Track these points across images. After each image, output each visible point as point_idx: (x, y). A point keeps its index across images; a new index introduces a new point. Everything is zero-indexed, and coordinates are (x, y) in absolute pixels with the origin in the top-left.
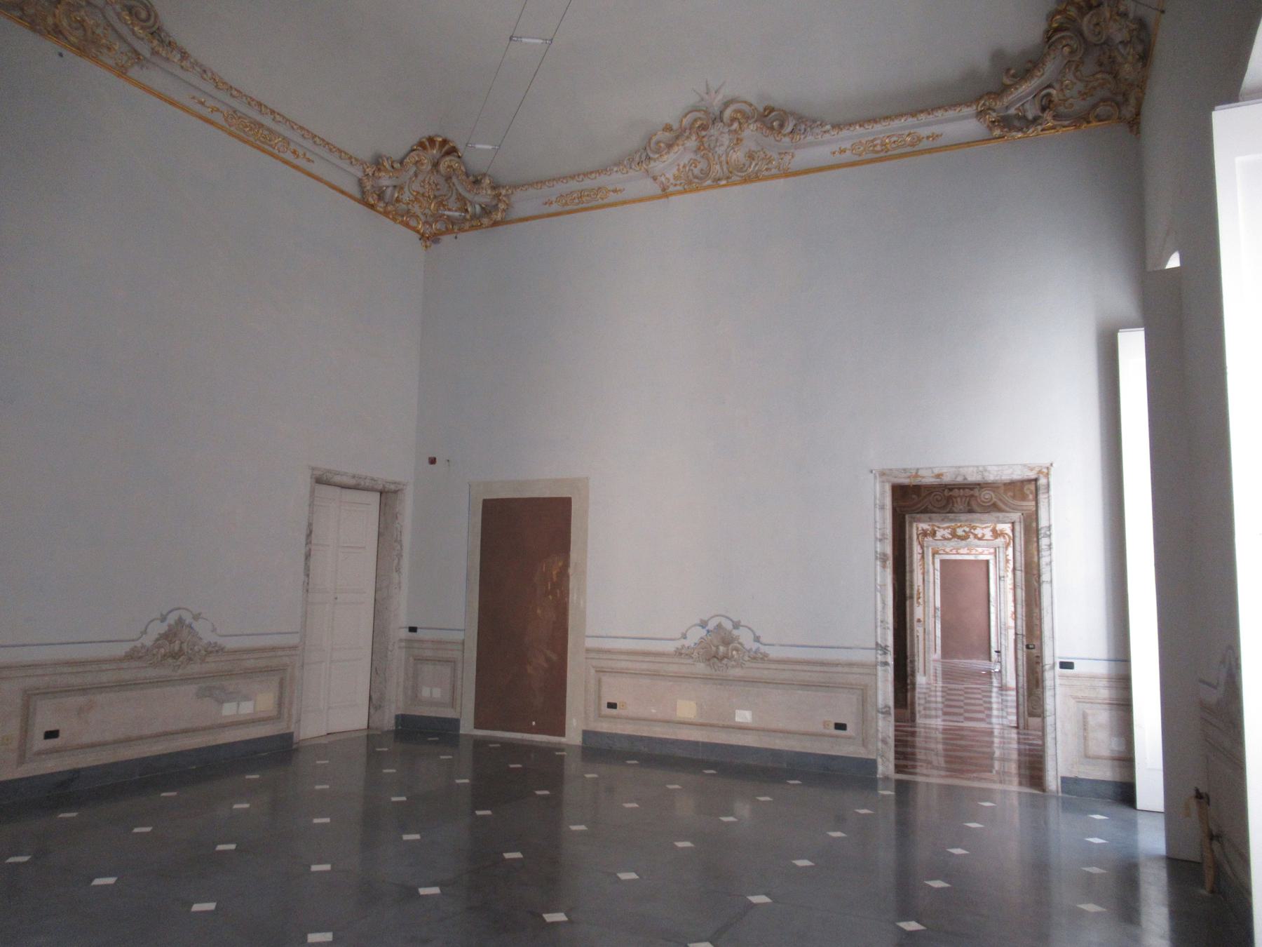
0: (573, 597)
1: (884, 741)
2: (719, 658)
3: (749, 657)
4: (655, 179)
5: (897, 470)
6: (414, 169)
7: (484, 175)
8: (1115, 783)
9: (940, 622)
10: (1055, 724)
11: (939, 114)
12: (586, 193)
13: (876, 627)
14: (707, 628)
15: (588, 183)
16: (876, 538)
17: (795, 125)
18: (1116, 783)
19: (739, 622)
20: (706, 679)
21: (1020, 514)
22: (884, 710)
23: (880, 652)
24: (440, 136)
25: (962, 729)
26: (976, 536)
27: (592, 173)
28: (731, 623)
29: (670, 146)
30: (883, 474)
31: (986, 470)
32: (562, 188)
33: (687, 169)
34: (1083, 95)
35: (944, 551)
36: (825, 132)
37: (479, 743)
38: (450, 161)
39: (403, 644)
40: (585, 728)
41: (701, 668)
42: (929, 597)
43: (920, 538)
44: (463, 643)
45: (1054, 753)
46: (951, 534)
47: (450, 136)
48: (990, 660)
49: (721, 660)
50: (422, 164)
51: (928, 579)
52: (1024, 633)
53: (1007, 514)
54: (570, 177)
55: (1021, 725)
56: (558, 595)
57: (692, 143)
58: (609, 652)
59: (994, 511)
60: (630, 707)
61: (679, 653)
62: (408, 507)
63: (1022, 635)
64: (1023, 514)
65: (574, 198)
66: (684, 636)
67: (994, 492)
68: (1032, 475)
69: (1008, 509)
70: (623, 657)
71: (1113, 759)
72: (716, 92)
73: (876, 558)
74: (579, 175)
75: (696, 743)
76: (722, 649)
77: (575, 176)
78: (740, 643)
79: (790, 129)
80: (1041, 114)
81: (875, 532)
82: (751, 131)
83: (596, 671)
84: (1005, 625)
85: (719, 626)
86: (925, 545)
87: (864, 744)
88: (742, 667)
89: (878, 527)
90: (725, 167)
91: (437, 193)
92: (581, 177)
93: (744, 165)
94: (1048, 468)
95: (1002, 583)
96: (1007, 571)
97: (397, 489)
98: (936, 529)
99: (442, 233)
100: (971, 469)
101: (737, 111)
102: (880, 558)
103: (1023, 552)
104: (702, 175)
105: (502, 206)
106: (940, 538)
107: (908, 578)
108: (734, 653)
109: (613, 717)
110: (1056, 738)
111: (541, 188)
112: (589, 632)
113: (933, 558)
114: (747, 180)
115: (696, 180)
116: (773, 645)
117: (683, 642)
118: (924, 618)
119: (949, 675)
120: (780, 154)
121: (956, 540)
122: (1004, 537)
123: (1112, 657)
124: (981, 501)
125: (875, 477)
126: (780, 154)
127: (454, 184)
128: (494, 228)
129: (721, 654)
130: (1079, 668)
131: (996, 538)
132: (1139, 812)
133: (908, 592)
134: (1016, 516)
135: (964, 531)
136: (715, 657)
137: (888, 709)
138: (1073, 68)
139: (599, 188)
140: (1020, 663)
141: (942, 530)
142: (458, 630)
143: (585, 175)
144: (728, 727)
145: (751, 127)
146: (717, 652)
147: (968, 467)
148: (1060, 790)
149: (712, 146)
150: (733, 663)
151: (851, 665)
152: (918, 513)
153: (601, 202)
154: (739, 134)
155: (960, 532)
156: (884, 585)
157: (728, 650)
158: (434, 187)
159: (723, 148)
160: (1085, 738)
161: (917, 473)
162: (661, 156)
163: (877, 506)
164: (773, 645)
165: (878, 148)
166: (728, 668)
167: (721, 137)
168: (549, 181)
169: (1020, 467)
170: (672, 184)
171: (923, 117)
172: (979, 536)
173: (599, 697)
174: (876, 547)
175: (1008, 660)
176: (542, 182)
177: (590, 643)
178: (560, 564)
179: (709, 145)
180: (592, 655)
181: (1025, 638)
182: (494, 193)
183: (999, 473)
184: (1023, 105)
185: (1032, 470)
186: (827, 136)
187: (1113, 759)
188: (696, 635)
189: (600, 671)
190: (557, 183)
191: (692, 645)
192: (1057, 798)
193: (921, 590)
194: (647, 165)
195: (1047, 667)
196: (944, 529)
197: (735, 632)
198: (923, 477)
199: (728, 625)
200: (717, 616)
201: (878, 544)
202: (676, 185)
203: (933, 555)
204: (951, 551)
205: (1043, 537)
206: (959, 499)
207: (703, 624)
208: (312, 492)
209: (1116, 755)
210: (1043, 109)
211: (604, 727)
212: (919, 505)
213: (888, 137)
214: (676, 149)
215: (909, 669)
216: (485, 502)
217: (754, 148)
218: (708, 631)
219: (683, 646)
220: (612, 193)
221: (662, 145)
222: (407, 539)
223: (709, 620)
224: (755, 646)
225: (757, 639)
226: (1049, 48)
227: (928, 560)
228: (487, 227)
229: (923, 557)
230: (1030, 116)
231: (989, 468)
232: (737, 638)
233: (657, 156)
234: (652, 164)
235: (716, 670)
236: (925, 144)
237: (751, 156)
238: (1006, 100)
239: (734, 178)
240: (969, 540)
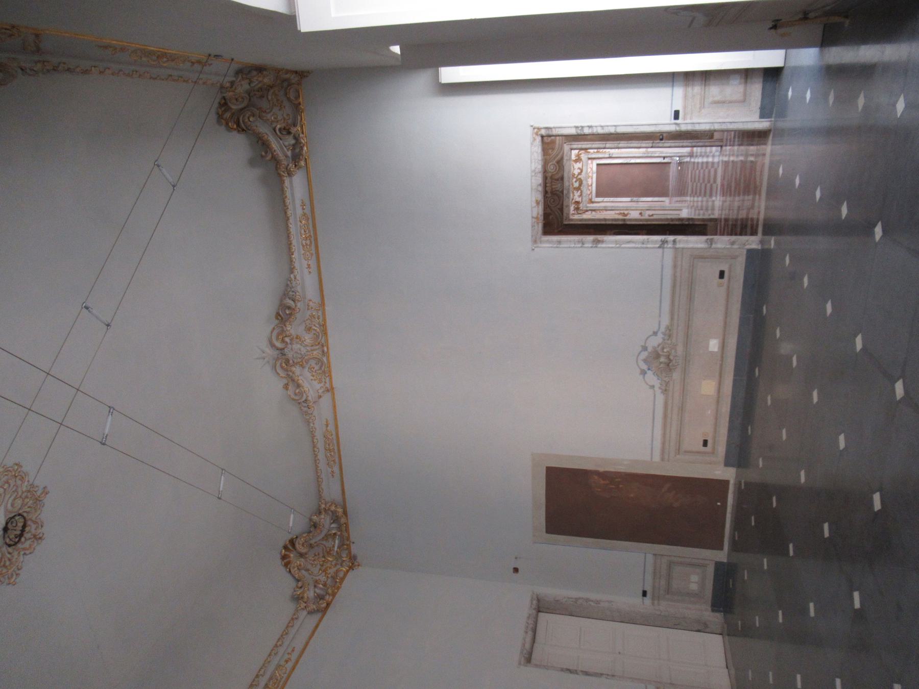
0: (622, 469)
1: (733, 243)
2: (668, 362)
3: (668, 340)
4: (320, 397)
5: (533, 230)
6: (303, 572)
7: (311, 520)
8: (765, 81)
10: (720, 123)
11: (288, 201)
12: (328, 447)
13: (647, 248)
14: (646, 370)
15: (320, 445)
16: (581, 247)
17: (289, 298)
18: (764, 81)
19: (642, 346)
20: (685, 371)
21: (565, 144)
22: (709, 243)
23: (666, 246)
24: (281, 552)
25: (722, 185)
26: (580, 174)
27: (313, 442)
28: (643, 353)
29: (299, 386)
30: (535, 242)
31: (535, 171)
32: (322, 465)
33: (314, 374)
34: (281, 107)
35: (589, 195)
36: (295, 278)
37: (735, 547)
38: (299, 544)
39: (656, 602)
40: (723, 465)
41: (676, 375)
42: (623, 207)
44: (655, 555)
45: (741, 123)
46: (578, 191)
47: (281, 544)
48: (670, 163)
49: (670, 361)
50: (300, 565)
51: (610, 207)
52: (652, 142)
53: (565, 152)
54: (315, 457)
55: (721, 144)
56: (619, 480)
57: (297, 370)
58: (663, 443)
59: (563, 162)
60: (706, 430)
61: (665, 391)
62: (551, 592)
63: (653, 143)
64: (565, 143)
65: (331, 455)
66: (653, 387)
67: (549, 163)
68: (539, 139)
69: (561, 153)
70: (668, 431)
71: (746, 82)
72: (264, 353)
73: (596, 247)
74: (314, 451)
75: (735, 381)
76: (662, 359)
77: (315, 454)
78: (659, 345)
79: (292, 303)
80: (292, 135)
81: (576, 247)
82: (293, 329)
83: (679, 454)
84: (645, 154)
85: (645, 361)
87: (734, 257)
88: (676, 345)
89: (574, 245)
90: (315, 348)
91: (321, 555)
92: (316, 449)
93: (314, 334)
94: (534, 129)
95: (614, 156)
97: (536, 599)
98: (574, 201)
99: (350, 552)
100: (533, 181)
101: (277, 339)
102: (596, 244)
103: (592, 143)
104: (320, 363)
105: (333, 508)
106: (581, 198)
107: (610, 223)
108: (665, 350)
109: (714, 443)
110: (731, 123)
111: (322, 479)
112: (648, 458)
114: (325, 333)
115: (323, 369)
116: (660, 322)
117: (656, 389)
118: (639, 210)
119: (681, 192)
120: (308, 309)
121: (582, 187)
122: (580, 154)
123: (671, 84)
124: (555, 171)
125: (538, 247)
126: (308, 309)
127: (316, 542)
128: (348, 515)
129: (666, 361)
130: (679, 107)
131: (581, 160)
132: (787, 65)
133: (621, 223)
134: (566, 147)
135: (576, 182)
136: (668, 365)
137: (708, 241)
138: (264, 114)
139: (325, 437)
140: (673, 145)
141: (575, 197)
142: (645, 558)
143: (314, 446)
144: (722, 357)
145: (289, 329)
146: (665, 363)
147: (532, 183)
148: (770, 119)
149: (300, 356)
150: (673, 351)
151: (675, 266)
152: (562, 214)
153: (334, 436)
154: (293, 337)
155: (576, 185)
156: (616, 242)
157: (663, 355)
158: (316, 557)
159: (302, 349)
160: (730, 102)
161: (535, 218)
162: (305, 392)
163: (558, 246)
164: (660, 322)
165: (308, 242)
166: (677, 356)
167: (295, 350)
168: (317, 473)
169: (532, 147)
170: (324, 385)
171: (289, 212)
172: (579, 171)
173: (698, 452)
174: (588, 247)
176: (318, 477)
177: (657, 458)
178: (596, 477)
179: (300, 358)
180: (666, 457)
181: (655, 142)
182: (324, 513)
183: (536, 161)
184: (286, 147)
185: (534, 139)
186: (298, 277)
187: (746, 82)
188: (651, 378)
189: (678, 451)
190: (319, 467)
191: (659, 381)
192: (776, 121)
194: (310, 402)
195: (678, 129)
196: (574, 195)
197: (650, 349)
198: (538, 214)
199: (644, 355)
200: (637, 362)
201: (586, 245)
202: (325, 382)
203: (593, 202)
204: (589, 190)
205: (583, 131)
206: (554, 187)
207: (643, 373)
208: (536, 666)
209: (743, 80)
210: (289, 133)
211: (722, 450)
212: (557, 214)
213: (301, 236)
214: (300, 382)
215: (677, 223)
216: (548, 531)
217: (302, 328)
218: (649, 369)
219: (660, 388)
220: (328, 428)
221: (297, 391)
222: (574, 594)
223: (640, 368)
224: (660, 336)
225: (655, 333)
226: (250, 130)
227: (596, 207)
228: (347, 519)
229: (594, 210)
230: (293, 142)
231: (533, 168)
232: (654, 348)
233: (304, 395)
234: (310, 398)
235: (678, 365)
236: (308, 211)
237: (309, 329)
238: (281, 156)
239: (323, 341)
240: (582, 178)
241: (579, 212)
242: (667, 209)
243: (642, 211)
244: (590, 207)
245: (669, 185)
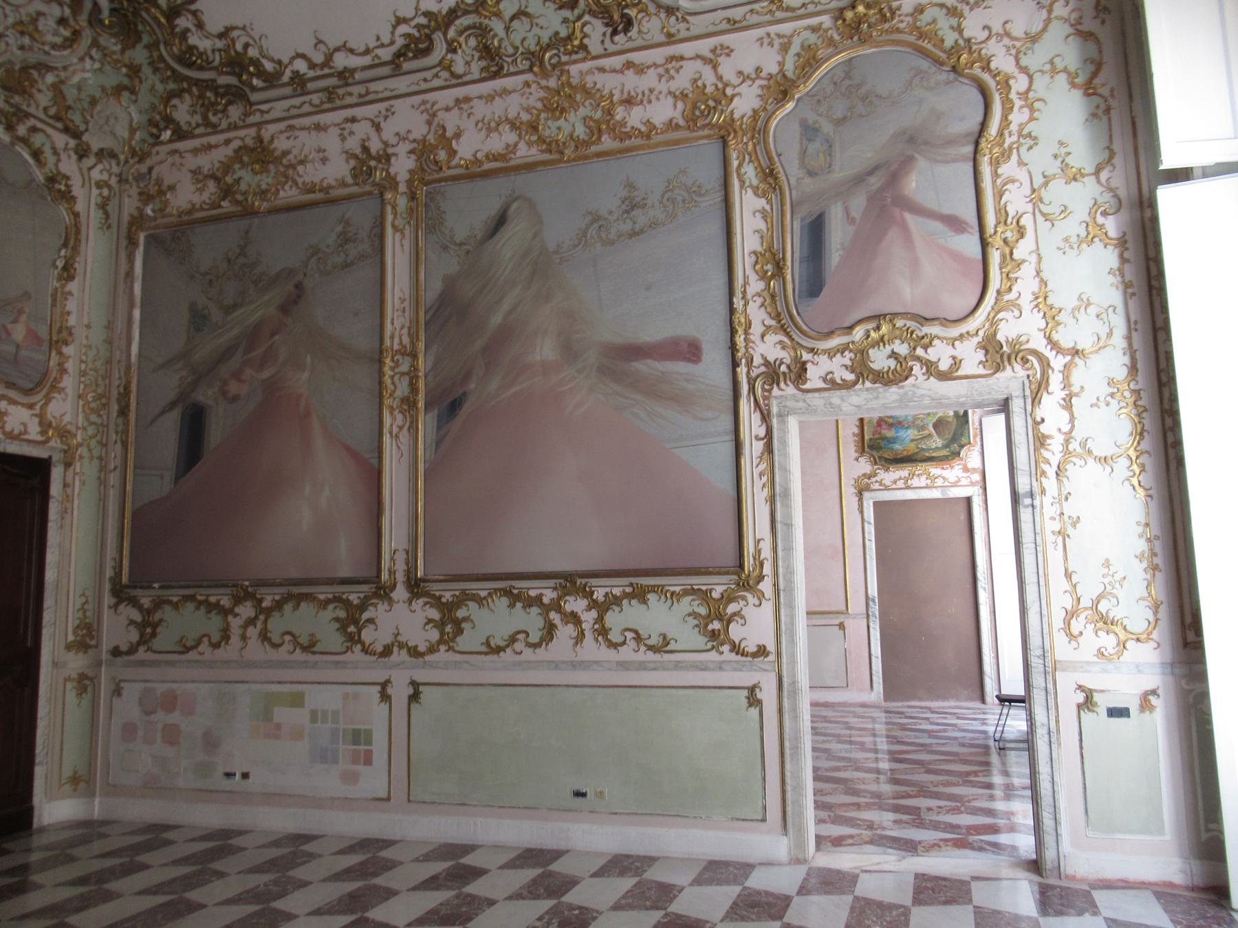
26: (931, 369)
35: (881, 483)
42: (790, 571)
43: (759, 391)
48: (983, 700)
51: (789, 516)
86: (775, 410)
95: (1025, 515)
96: (1043, 473)
98: (806, 356)
106: (822, 385)
113: (861, 500)
121: (868, 384)
122: (1025, 361)
131: (998, 368)
135: (894, 355)
141: (823, 359)
155: (880, 360)
172: (944, 366)
175: (1061, 780)
193: (766, 553)
196: (831, 354)
203: (860, 494)
229: (769, 448)
240: (911, 380)
241: (758, 385)
242: (788, 766)
243: (772, 658)
244: (784, 432)
245: (920, 699)
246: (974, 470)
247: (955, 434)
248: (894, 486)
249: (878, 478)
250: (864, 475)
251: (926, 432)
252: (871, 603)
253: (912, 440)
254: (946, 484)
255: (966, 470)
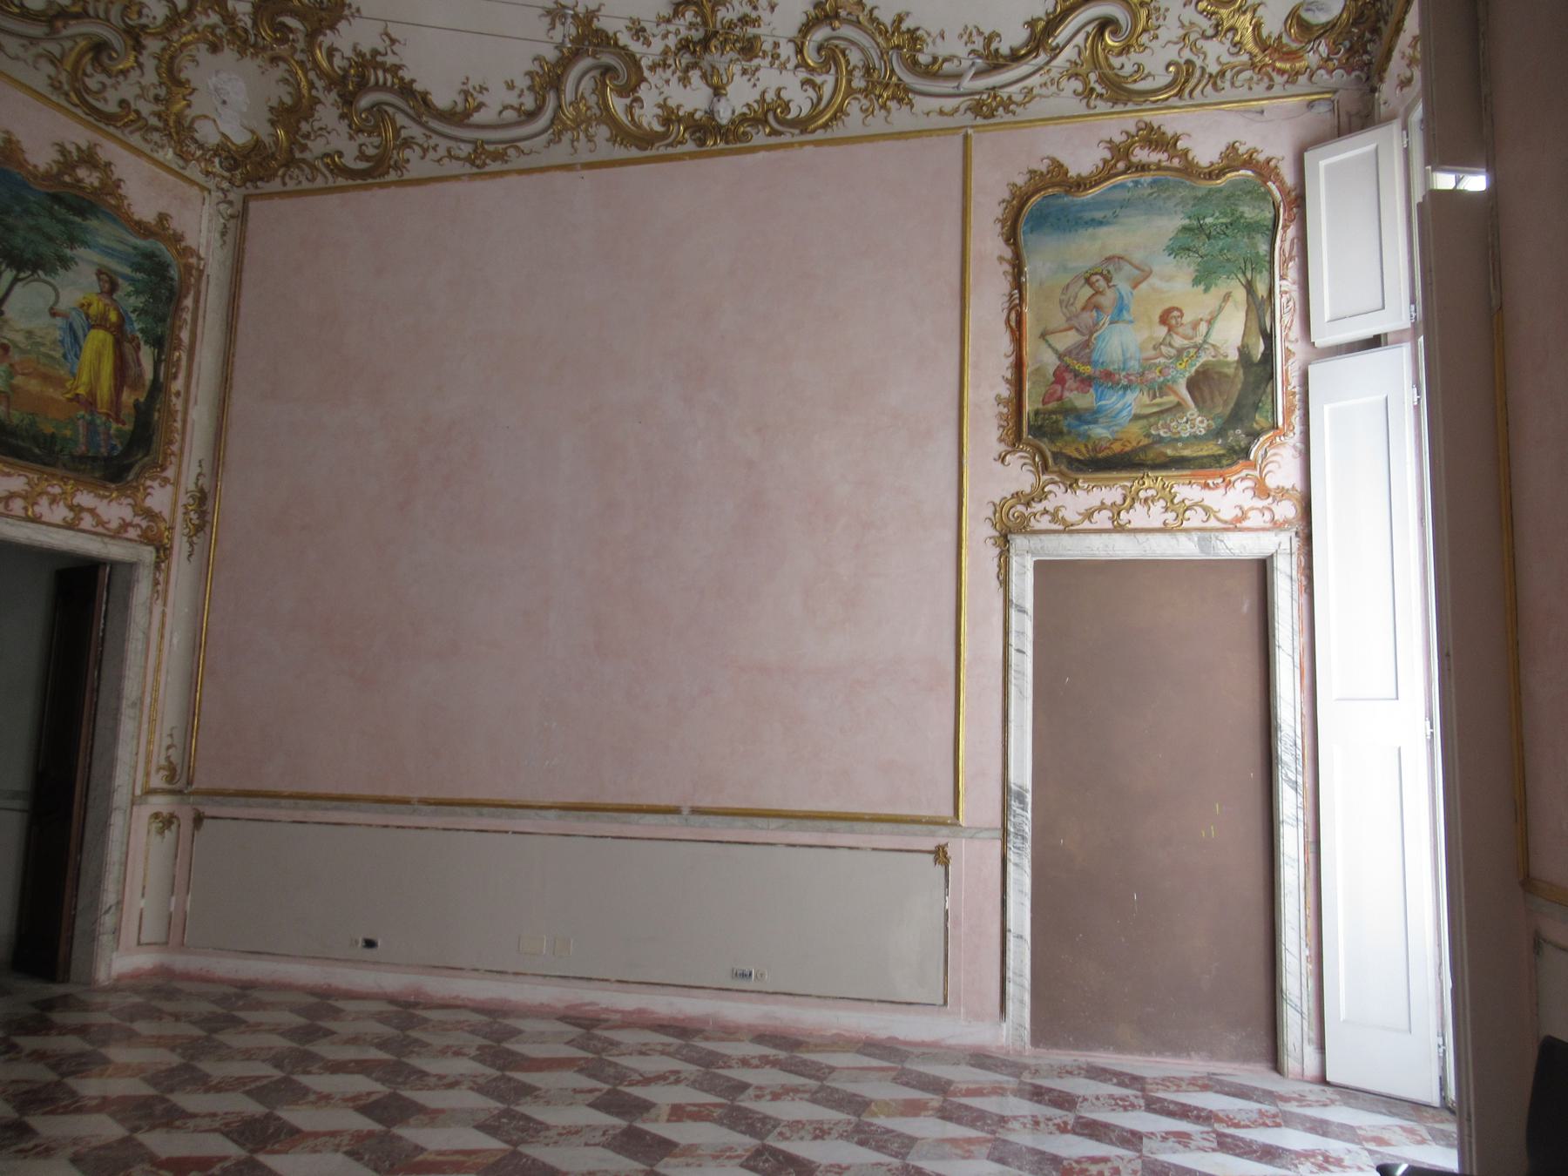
9: (1027, 863)
35: (1054, 517)
48: (1275, 1060)
203: (1004, 541)
204: (1089, 515)
245: (1121, 1048)
246: (1282, 493)
247: (1238, 405)
248: (1086, 525)
249: (1049, 504)
250: (1016, 495)
251: (1170, 399)
252: (1014, 805)
253: (1137, 417)
254: (1213, 523)
255: (1261, 490)
